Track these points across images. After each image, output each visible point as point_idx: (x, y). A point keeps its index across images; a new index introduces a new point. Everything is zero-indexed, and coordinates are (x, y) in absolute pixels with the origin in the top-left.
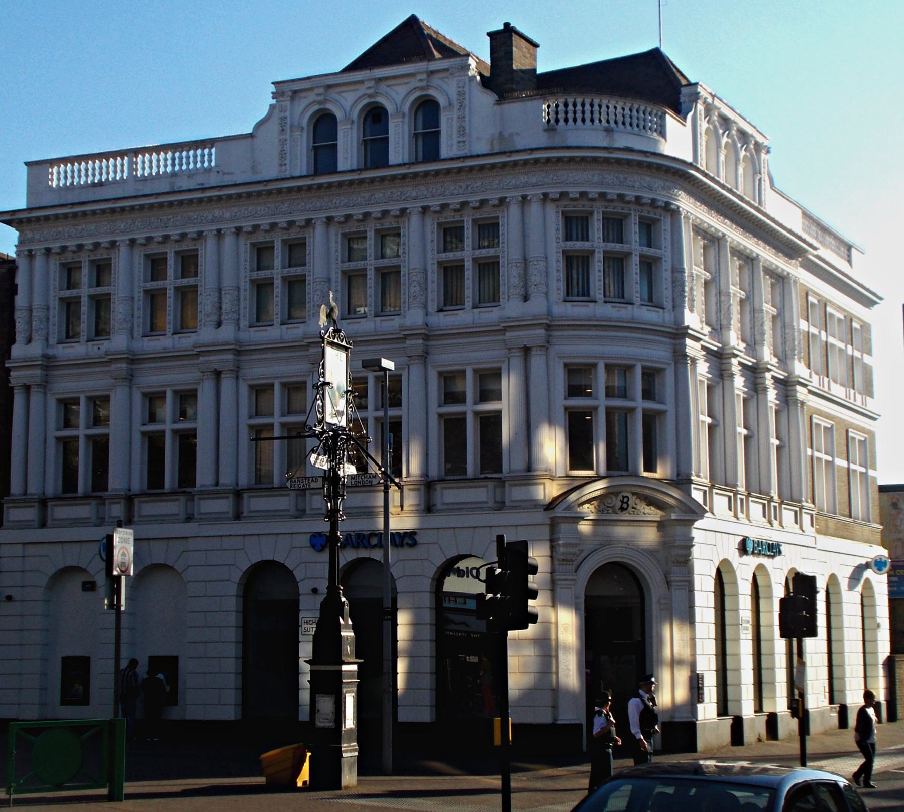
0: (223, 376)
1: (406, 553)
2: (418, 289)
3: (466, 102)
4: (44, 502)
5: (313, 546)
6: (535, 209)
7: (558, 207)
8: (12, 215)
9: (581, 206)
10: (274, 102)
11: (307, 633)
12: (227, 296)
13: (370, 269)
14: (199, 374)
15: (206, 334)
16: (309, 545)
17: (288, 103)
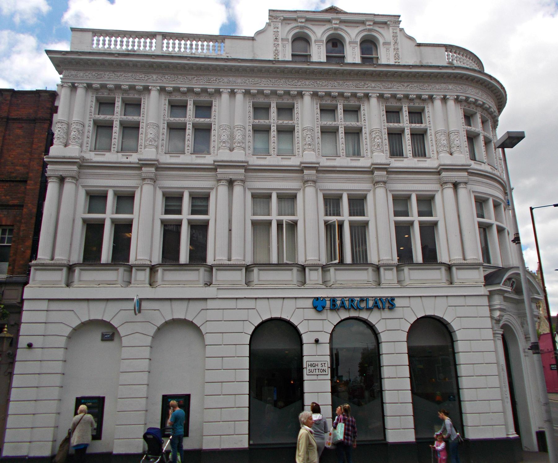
0: (235, 183)
1: (386, 314)
2: (380, 140)
3: (399, 41)
4: (71, 268)
5: (315, 308)
6: (451, 103)
7: (461, 106)
8: (64, 55)
9: (472, 109)
10: (268, 21)
11: (311, 373)
12: (239, 131)
13: (341, 127)
14: (215, 182)
15: (224, 155)
16: (311, 306)
17: (280, 24)
